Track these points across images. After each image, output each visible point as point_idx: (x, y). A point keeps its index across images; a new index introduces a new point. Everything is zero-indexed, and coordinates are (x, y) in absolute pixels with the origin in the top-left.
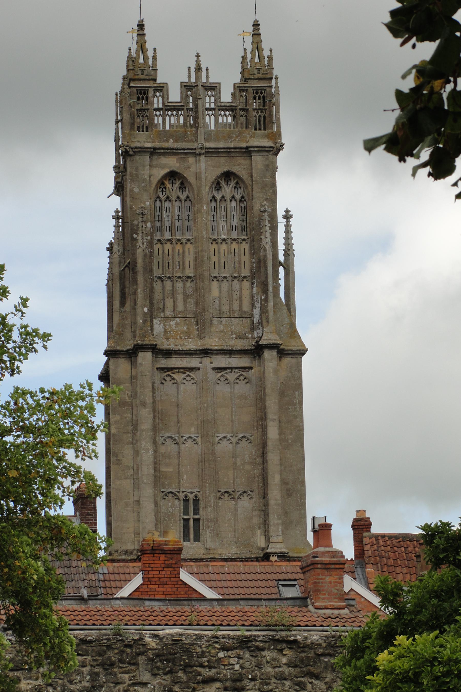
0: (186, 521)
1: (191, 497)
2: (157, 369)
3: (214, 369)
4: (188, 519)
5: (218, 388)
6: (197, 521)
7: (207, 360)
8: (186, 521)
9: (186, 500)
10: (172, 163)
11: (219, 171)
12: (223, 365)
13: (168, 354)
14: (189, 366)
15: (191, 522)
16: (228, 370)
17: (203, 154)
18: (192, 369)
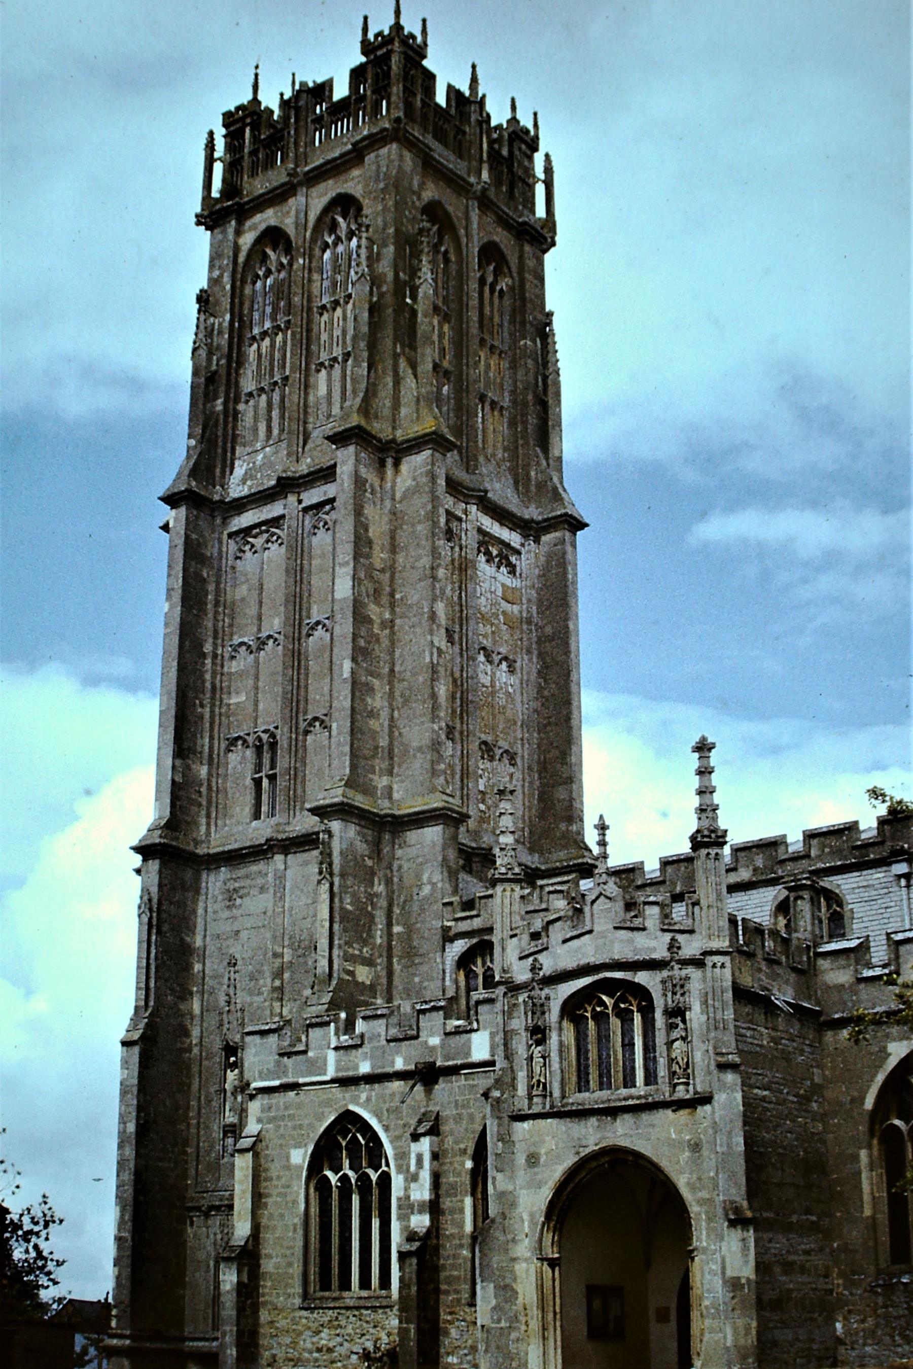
0: (258, 783)
1: (265, 737)
2: (230, 536)
3: (306, 510)
4: (261, 778)
5: (315, 540)
6: (272, 778)
7: (292, 499)
8: (258, 783)
9: (259, 749)
10: (267, 218)
11: (325, 200)
12: (315, 500)
13: (240, 505)
14: (270, 516)
15: (265, 783)
16: (328, 507)
17: (300, 184)
18: (276, 521)
